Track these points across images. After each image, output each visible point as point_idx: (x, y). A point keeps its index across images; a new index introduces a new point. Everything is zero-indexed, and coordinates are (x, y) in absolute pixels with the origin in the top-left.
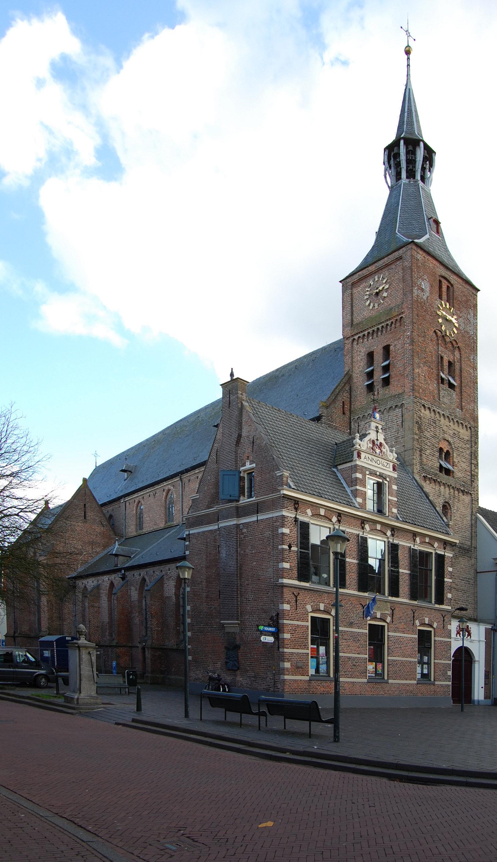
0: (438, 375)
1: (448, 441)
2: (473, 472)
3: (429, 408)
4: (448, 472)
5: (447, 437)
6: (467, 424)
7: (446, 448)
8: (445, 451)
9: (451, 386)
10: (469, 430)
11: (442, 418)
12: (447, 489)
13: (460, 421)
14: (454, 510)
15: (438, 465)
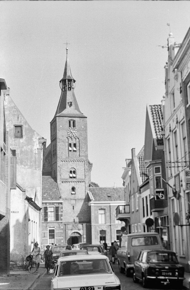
0: (68, 149)
1: (73, 168)
2: (86, 175)
3: (64, 161)
4: (74, 177)
5: (72, 167)
6: (82, 160)
7: (73, 170)
8: (73, 171)
9: (75, 151)
10: (84, 162)
11: (70, 162)
12: (73, 183)
13: (78, 161)
14: (76, 189)
15: (69, 176)
